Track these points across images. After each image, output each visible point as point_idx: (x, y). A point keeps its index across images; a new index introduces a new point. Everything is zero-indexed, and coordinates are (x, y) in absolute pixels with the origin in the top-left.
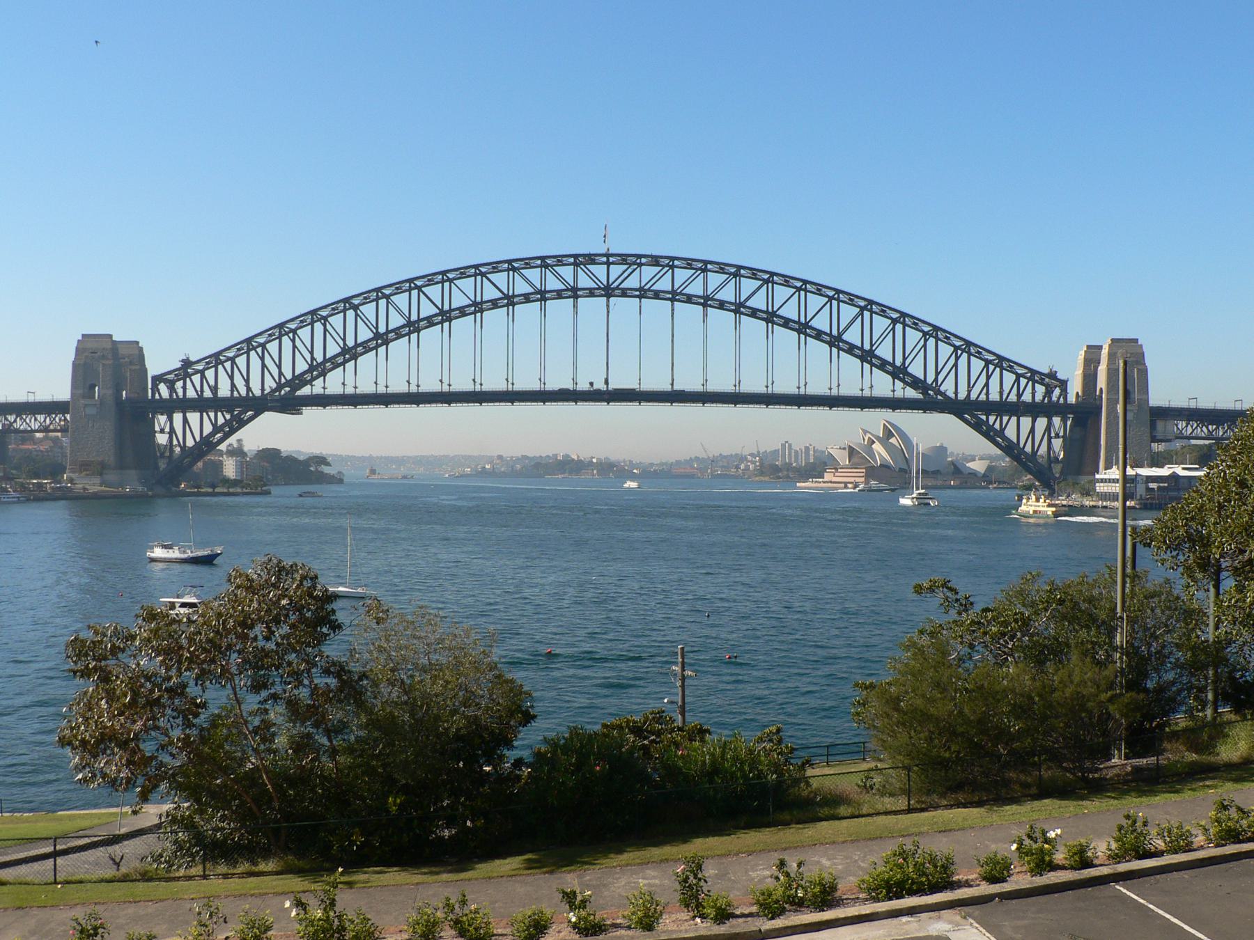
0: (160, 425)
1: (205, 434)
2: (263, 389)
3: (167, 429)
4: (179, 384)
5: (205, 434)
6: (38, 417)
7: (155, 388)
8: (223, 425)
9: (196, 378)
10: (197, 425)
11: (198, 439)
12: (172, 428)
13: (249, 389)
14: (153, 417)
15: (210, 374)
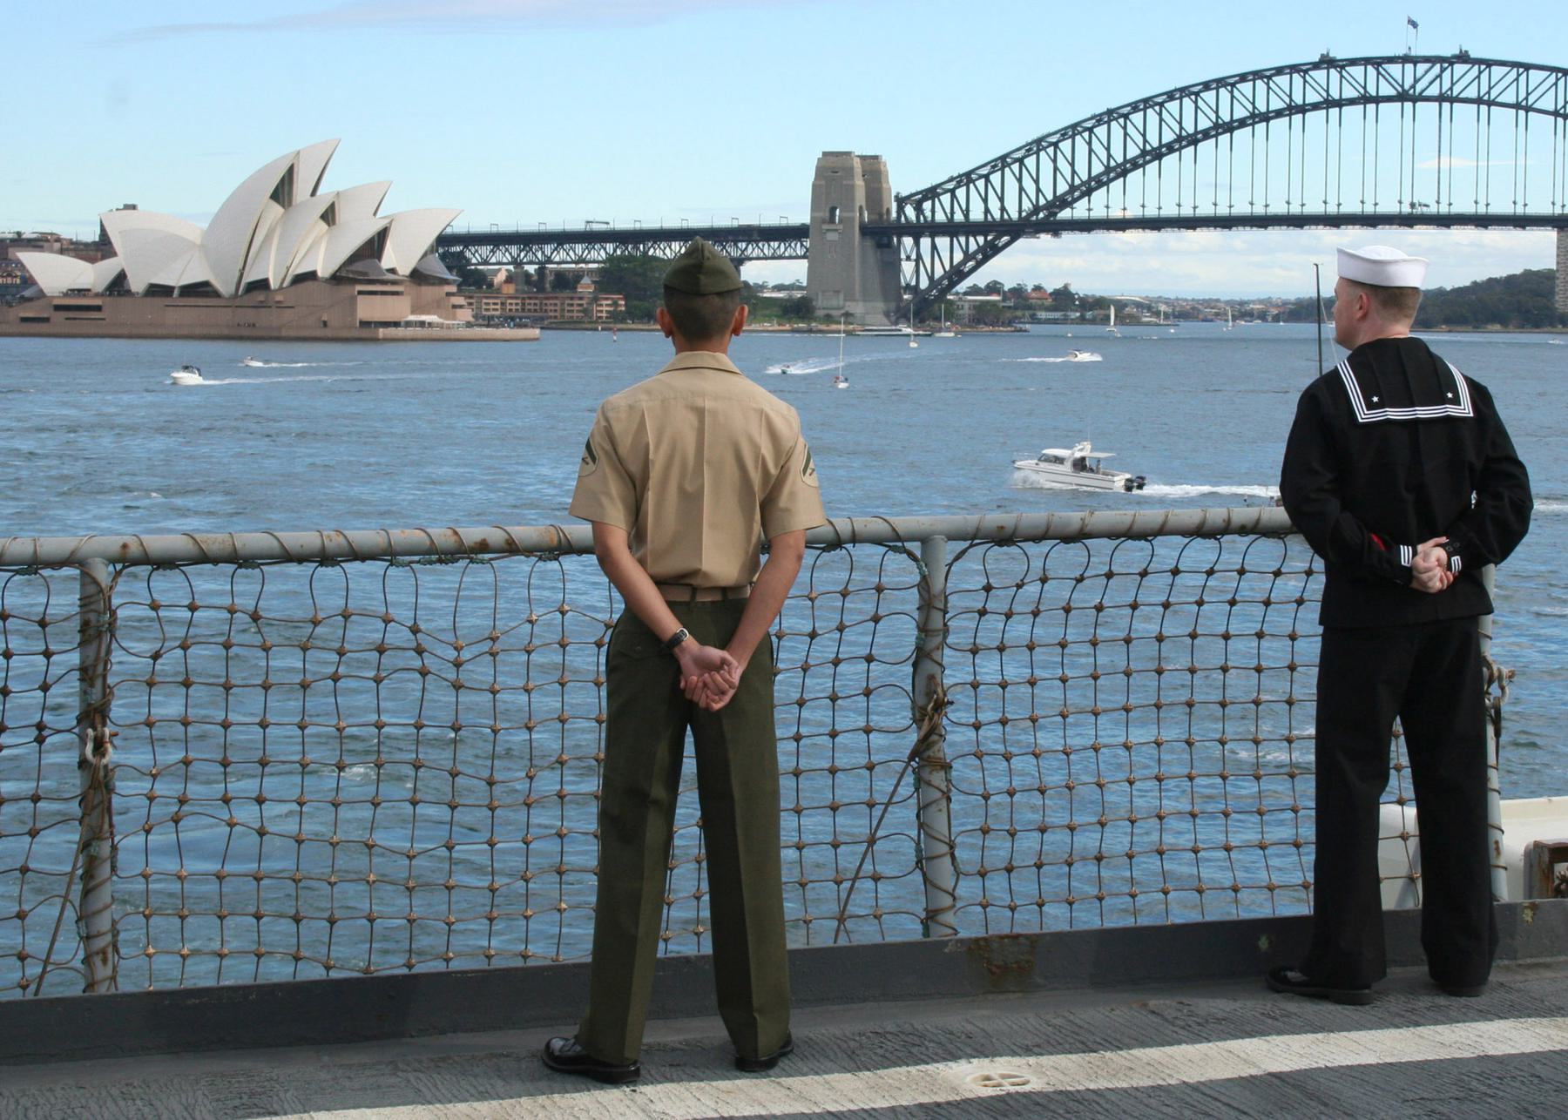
0: (905, 251)
1: (955, 263)
2: (1020, 211)
3: (914, 256)
4: (927, 205)
5: (955, 262)
6: (772, 244)
7: (901, 209)
8: (976, 252)
9: (946, 198)
10: (948, 251)
11: (947, 268)
12: (919, 257)
13: (1003, 209)
14: (899, 242)
15: (961, 193)
